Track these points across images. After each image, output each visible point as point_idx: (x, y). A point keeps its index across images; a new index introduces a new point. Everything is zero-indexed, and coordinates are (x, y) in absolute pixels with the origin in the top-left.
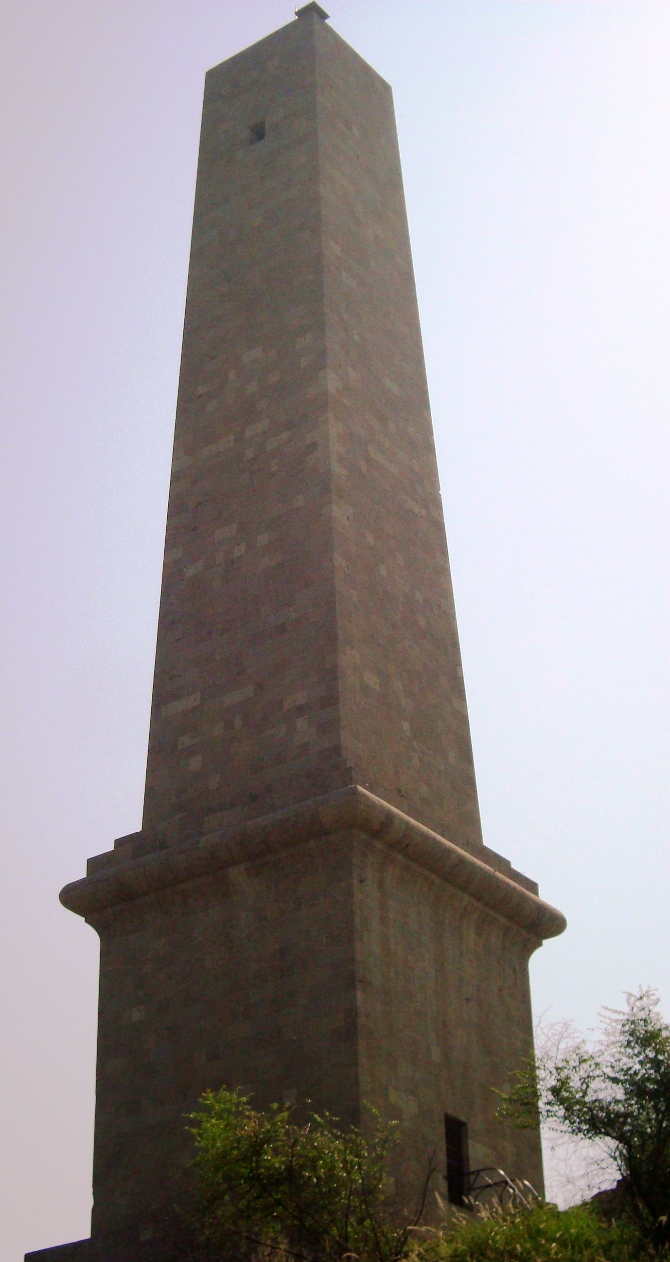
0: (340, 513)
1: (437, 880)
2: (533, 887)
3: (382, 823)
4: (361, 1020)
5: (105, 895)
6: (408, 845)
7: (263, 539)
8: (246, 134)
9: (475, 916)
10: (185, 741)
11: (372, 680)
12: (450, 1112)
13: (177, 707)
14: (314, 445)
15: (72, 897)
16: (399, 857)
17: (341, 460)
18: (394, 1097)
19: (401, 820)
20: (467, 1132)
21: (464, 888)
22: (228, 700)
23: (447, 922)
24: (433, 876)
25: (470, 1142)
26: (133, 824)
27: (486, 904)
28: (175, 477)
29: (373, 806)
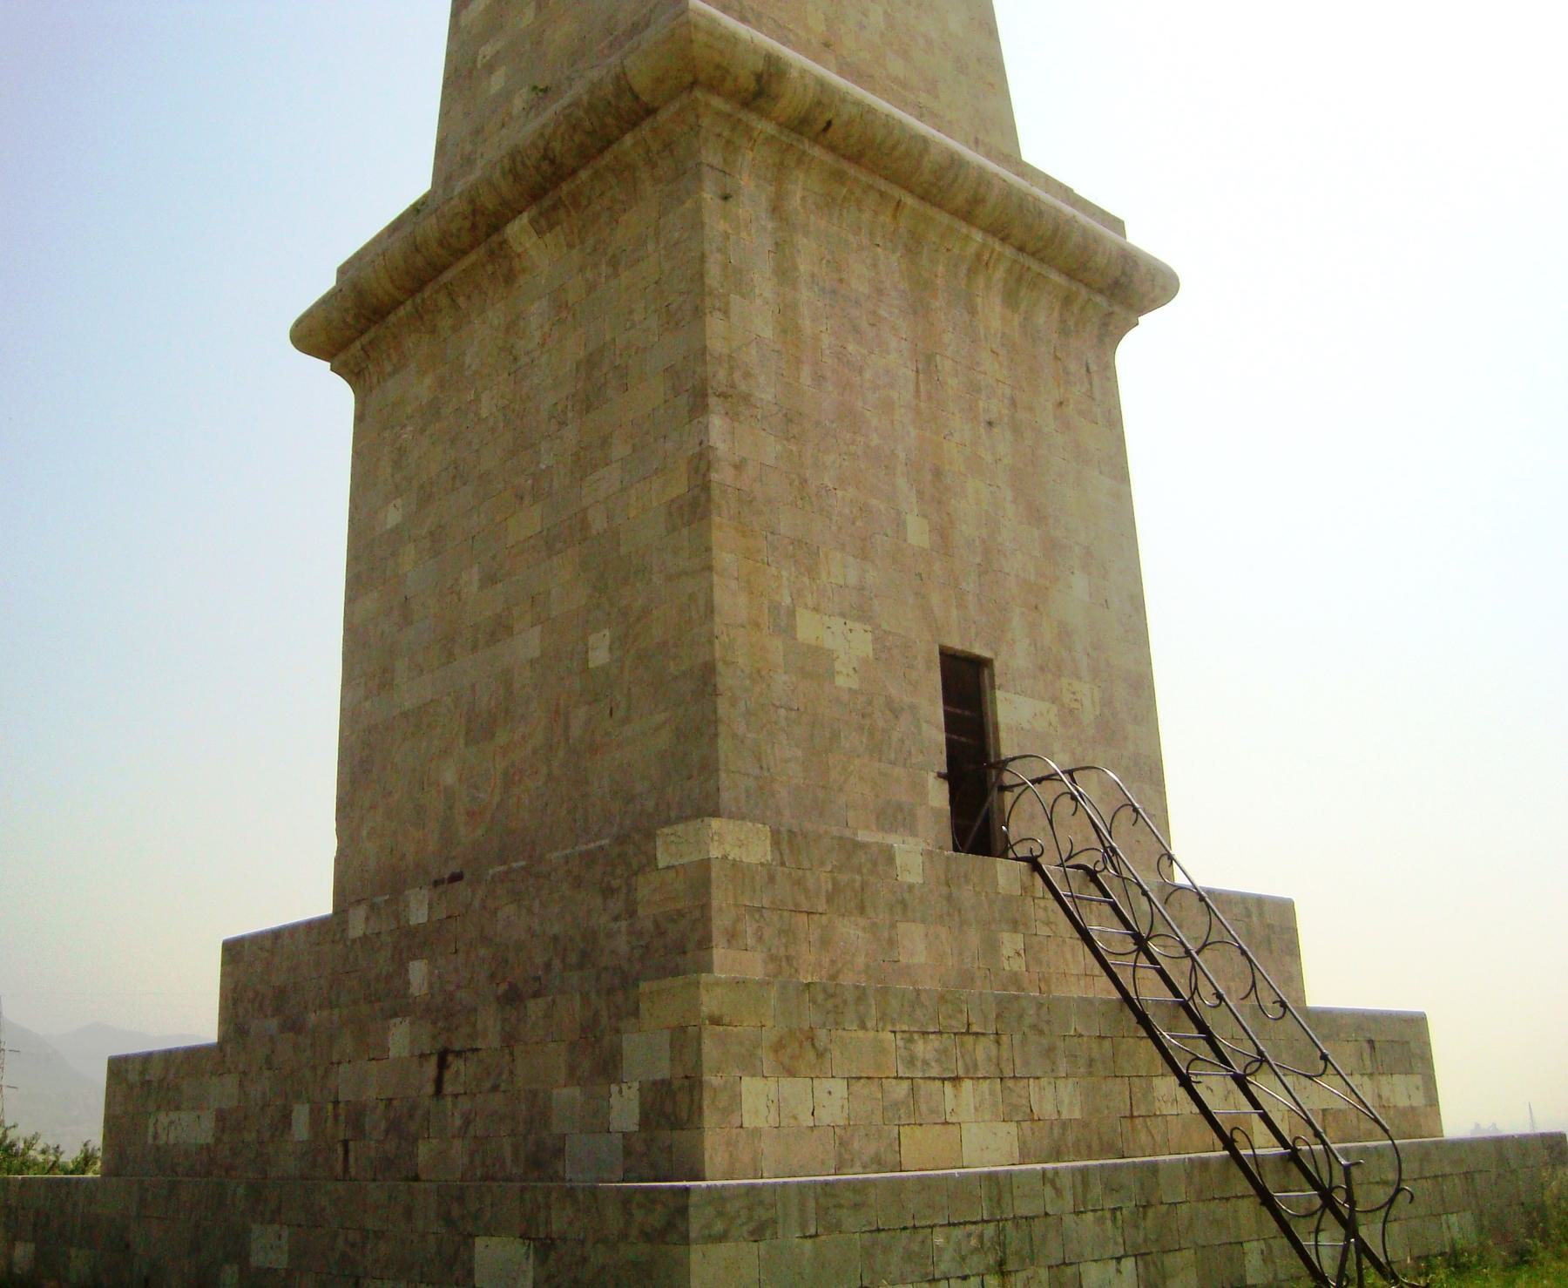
1: (909, 201)
2: (1117, 225)
3: (759, 77)
4: (721, 476)
6: (829, 124)
9: (999, 274)
10: (488, 50)
12: (956, 643)
16: (817, 152)
18: (808, 628)
19: (803, 72)
20: (992, 676)
23: (939, 282)
24: (897, 193)
25: (999, 694)
27: (1021, 249)
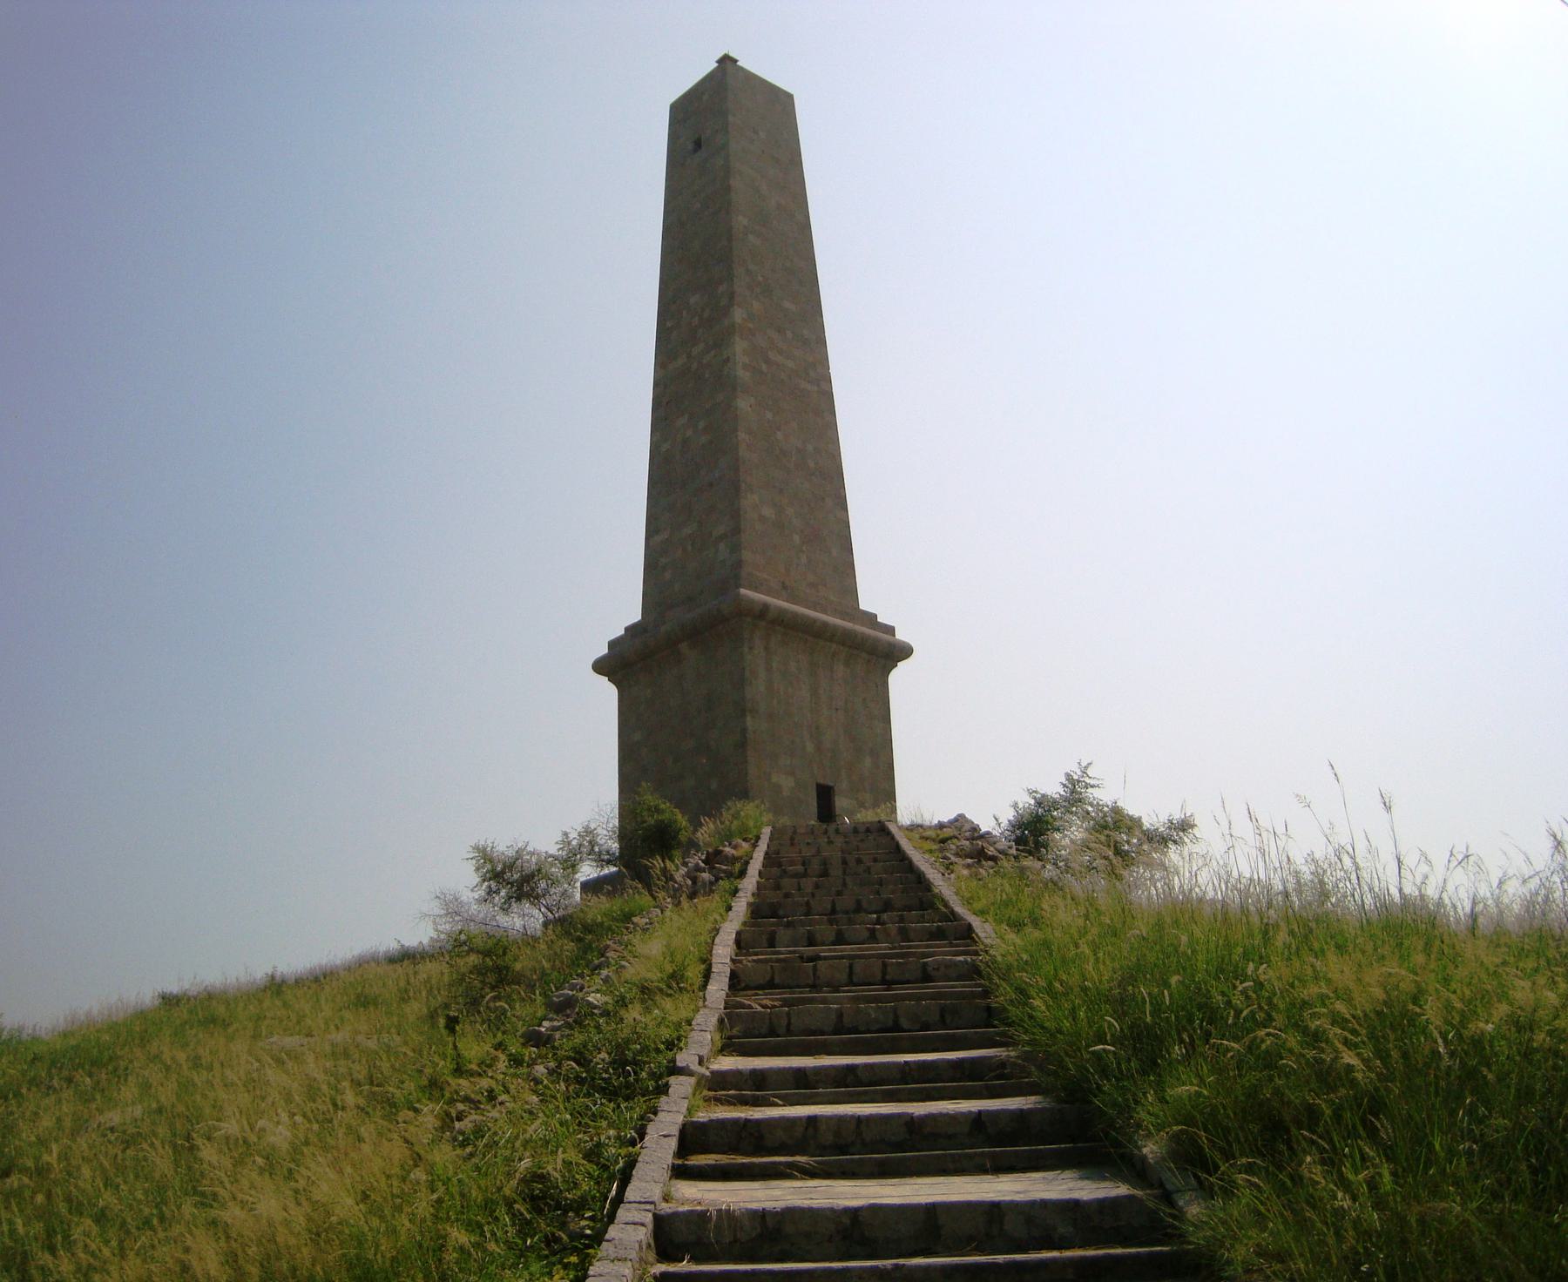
0: (744, 404)
2: (890, 630)
7: (701, 425)
8: (690, 147)
10: (663, 560)
11: (768, 512)
13: (658, 538)
14: (728, 359)
15: (600, 667)
17: (745, 367)
18: (774, 779)
21: (831, 639)
22: (687, 531)
26: (635, 615)
28: (657, 384)
29: (752, 601)
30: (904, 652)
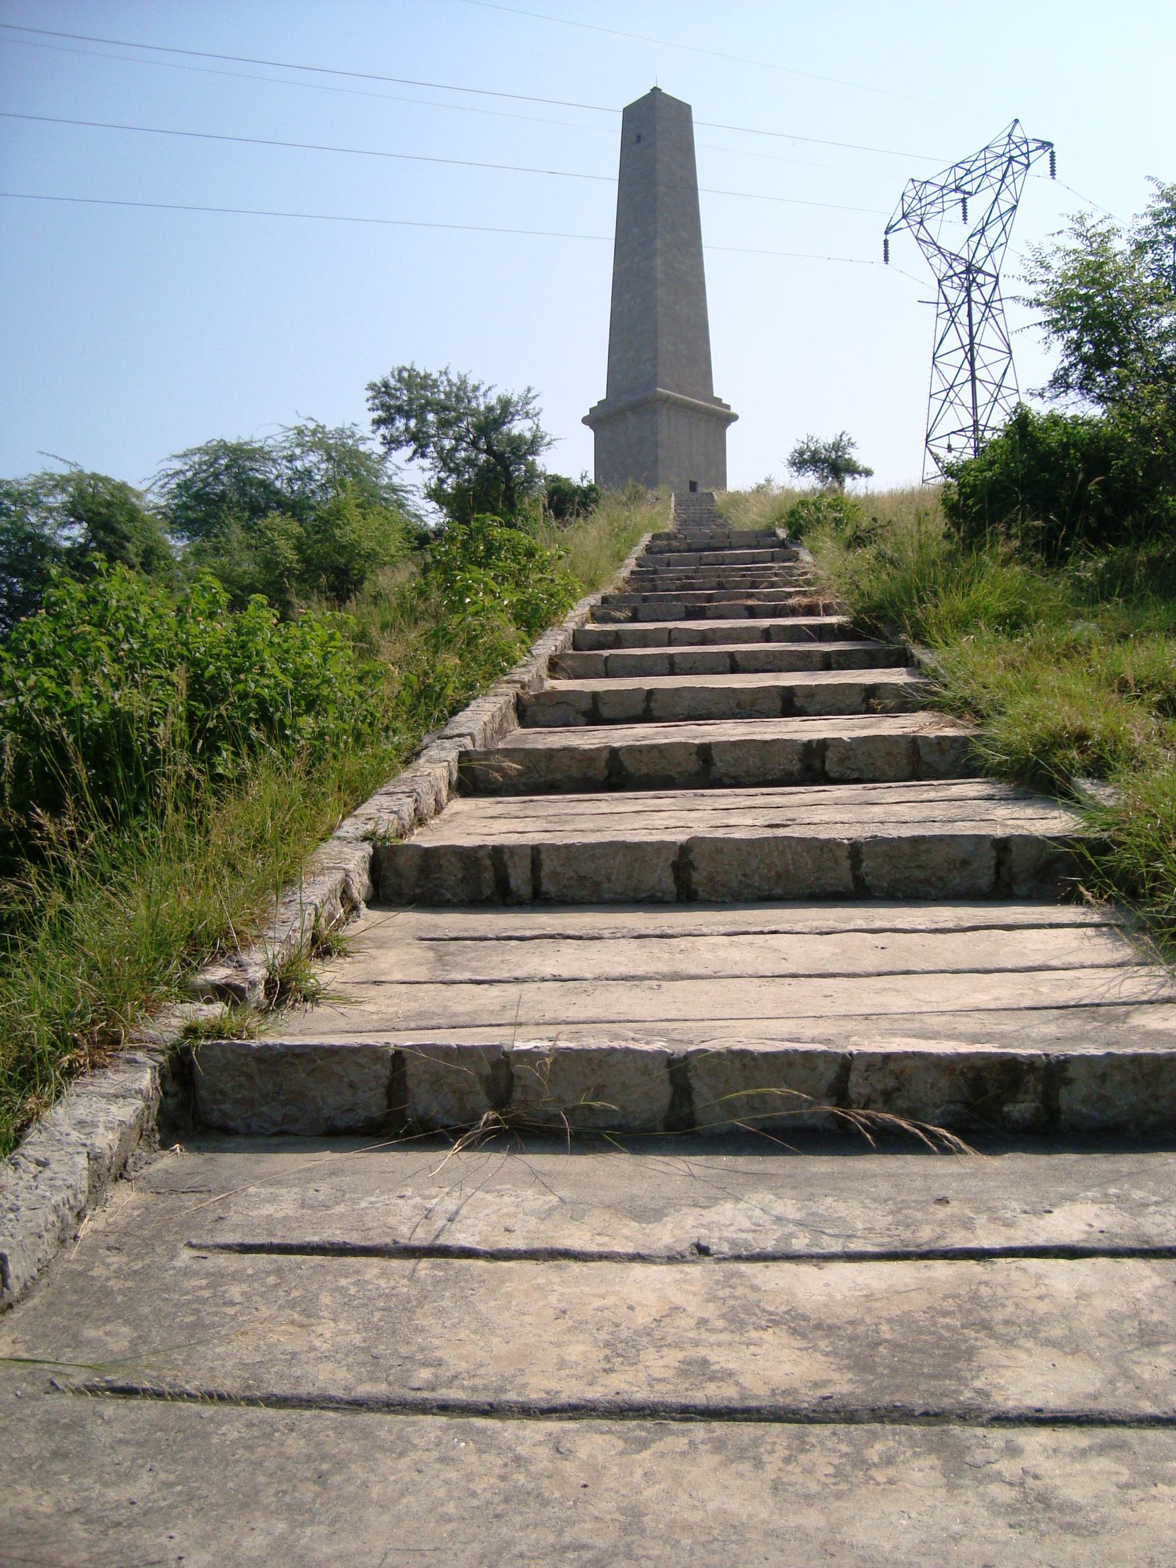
0: (660, 292)
2: (728, 407)
5: (594, 420)
8: (634, 138)
30: (735, 418)
